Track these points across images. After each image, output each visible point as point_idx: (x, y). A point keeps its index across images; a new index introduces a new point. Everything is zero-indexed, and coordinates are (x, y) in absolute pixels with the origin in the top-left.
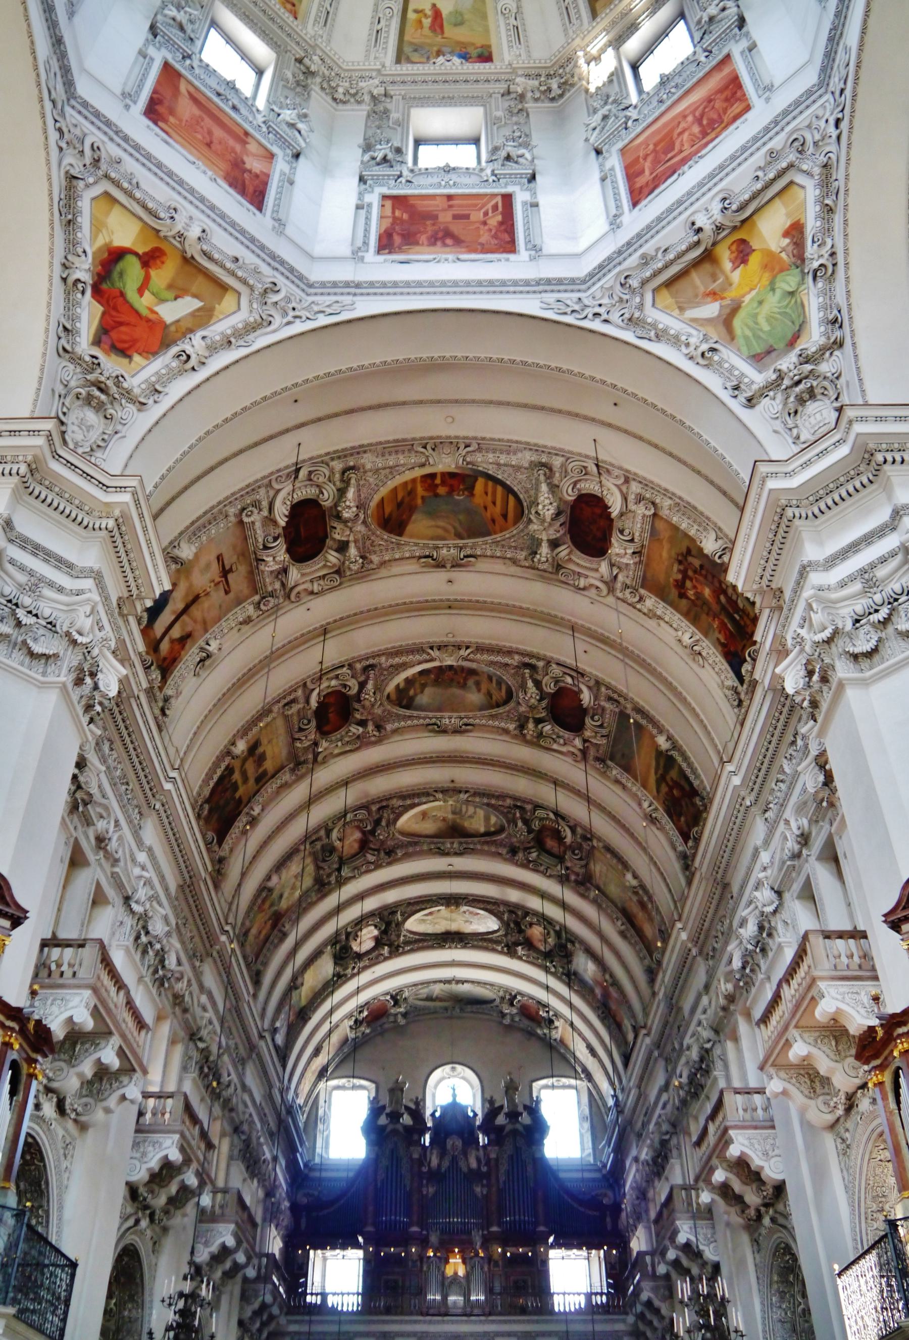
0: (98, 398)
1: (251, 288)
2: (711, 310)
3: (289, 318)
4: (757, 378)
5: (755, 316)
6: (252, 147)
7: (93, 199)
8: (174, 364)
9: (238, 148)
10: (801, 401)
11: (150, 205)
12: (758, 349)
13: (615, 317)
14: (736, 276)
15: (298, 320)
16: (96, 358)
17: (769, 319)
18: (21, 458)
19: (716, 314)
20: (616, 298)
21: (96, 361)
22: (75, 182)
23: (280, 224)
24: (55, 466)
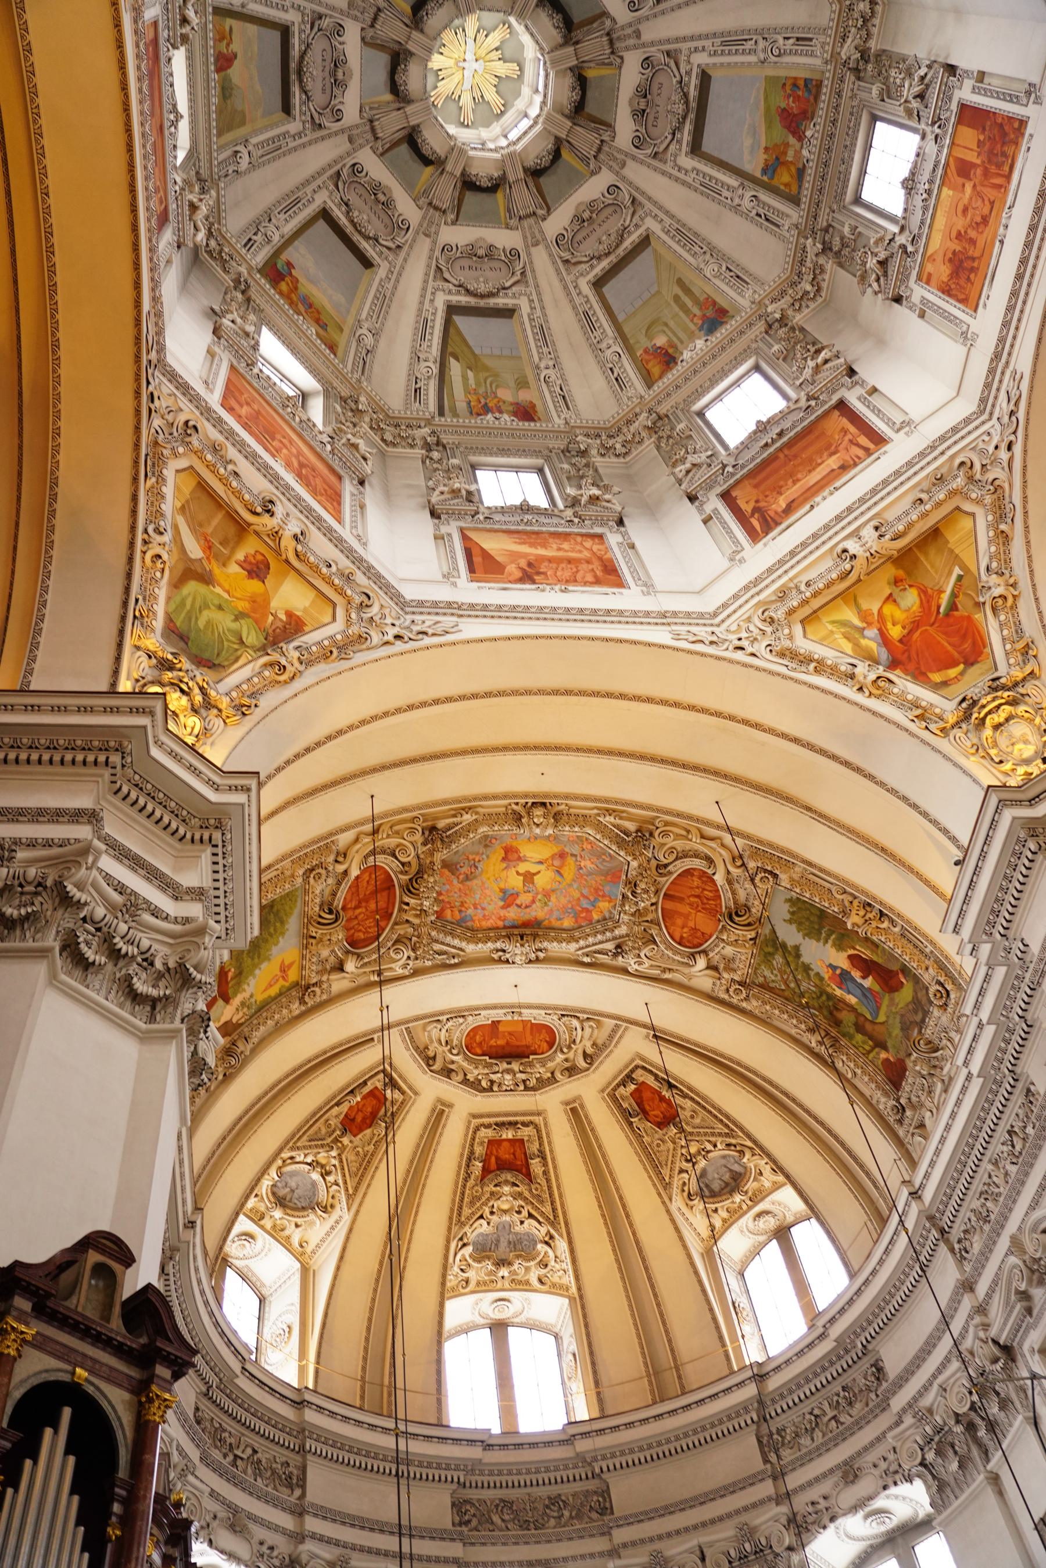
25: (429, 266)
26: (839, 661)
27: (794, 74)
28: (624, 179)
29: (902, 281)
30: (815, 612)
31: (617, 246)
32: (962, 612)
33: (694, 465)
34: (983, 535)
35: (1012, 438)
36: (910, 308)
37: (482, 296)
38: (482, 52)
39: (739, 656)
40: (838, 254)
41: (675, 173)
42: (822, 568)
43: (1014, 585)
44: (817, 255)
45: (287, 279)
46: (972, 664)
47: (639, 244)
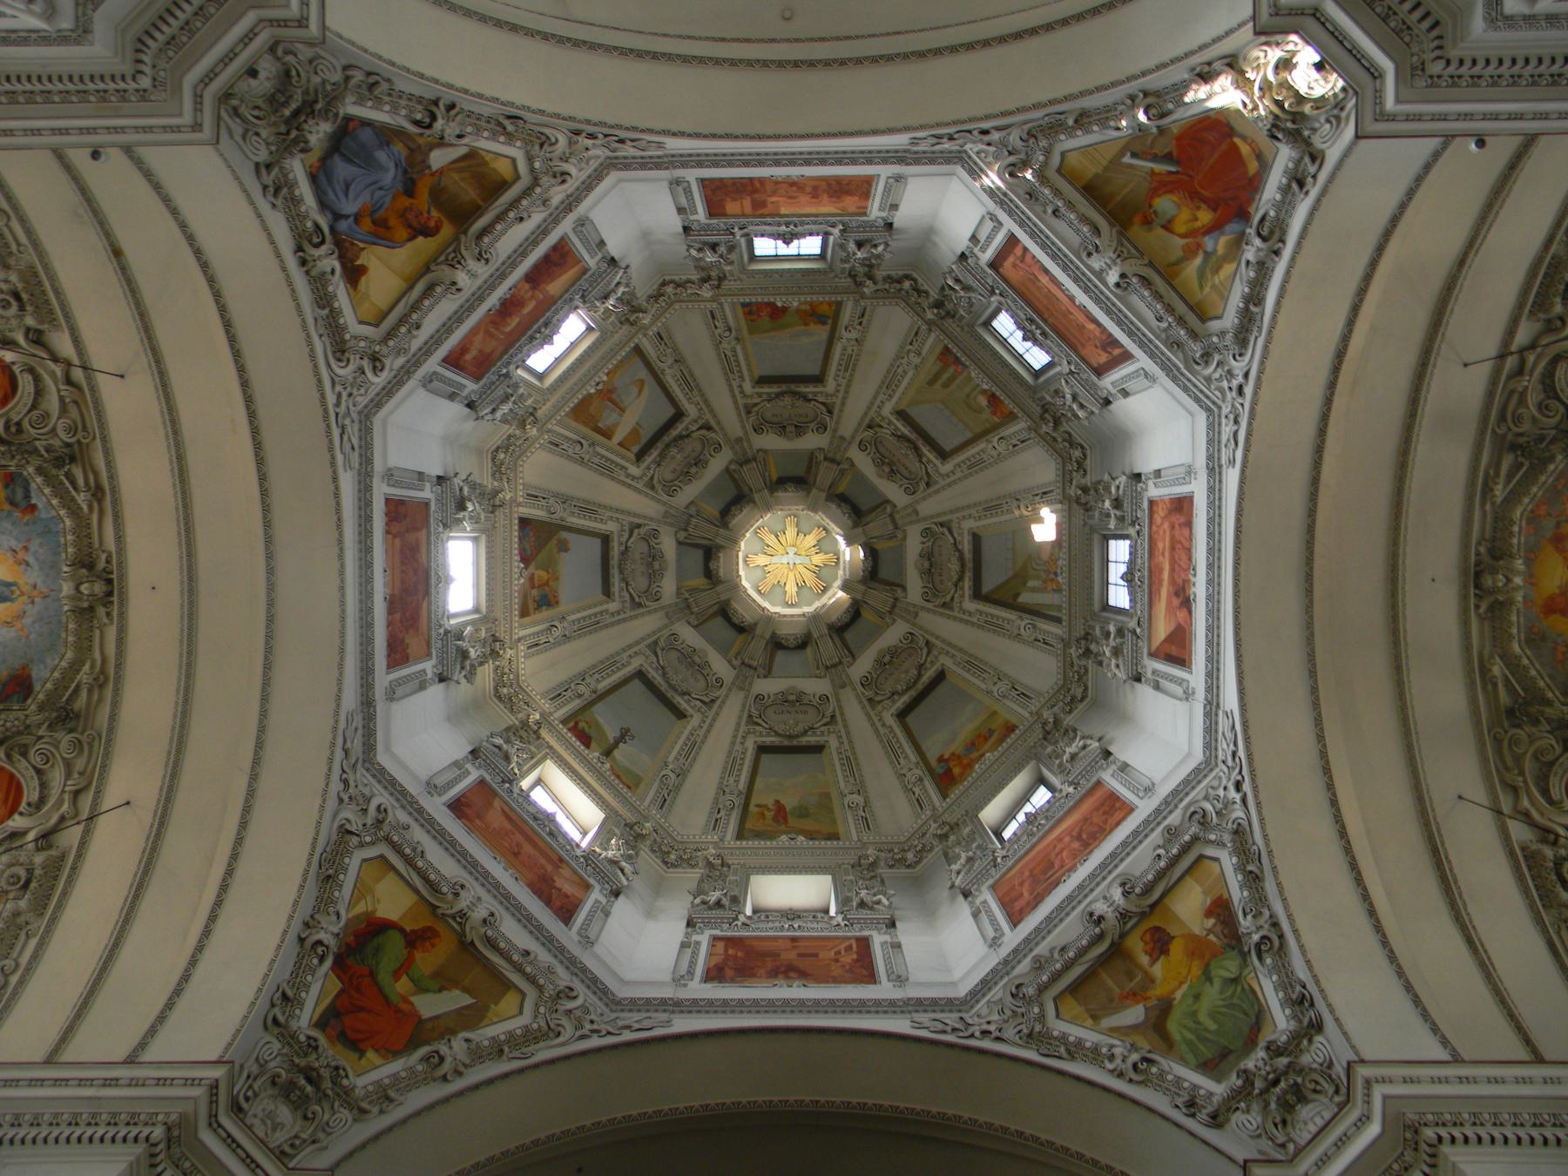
0: (302, 1089)
1: (540, 988)
2: (1134, 1014)
3: (585, 1031)
4: (1215, 1089)
5: (1193, 1015)
6: (565, 872)
7: (364, 860)
8: (420, 1068)
9: (549, 868)
10: (1287, 1107)
11: (432, 877)
12: (1207, 1053)
13: (1010, 1033)
14: (1157, 970)
15: (595, 1035)
16: (315, 1040)
17: (1213, 1015)
18: (160, 1117)
19: (1142, 1018)
20: (1008, 1013)
21: (313, 1044)
22: (348, 837)
23: (588, 942)
24: (208, 1138)
33: (1075, 397)
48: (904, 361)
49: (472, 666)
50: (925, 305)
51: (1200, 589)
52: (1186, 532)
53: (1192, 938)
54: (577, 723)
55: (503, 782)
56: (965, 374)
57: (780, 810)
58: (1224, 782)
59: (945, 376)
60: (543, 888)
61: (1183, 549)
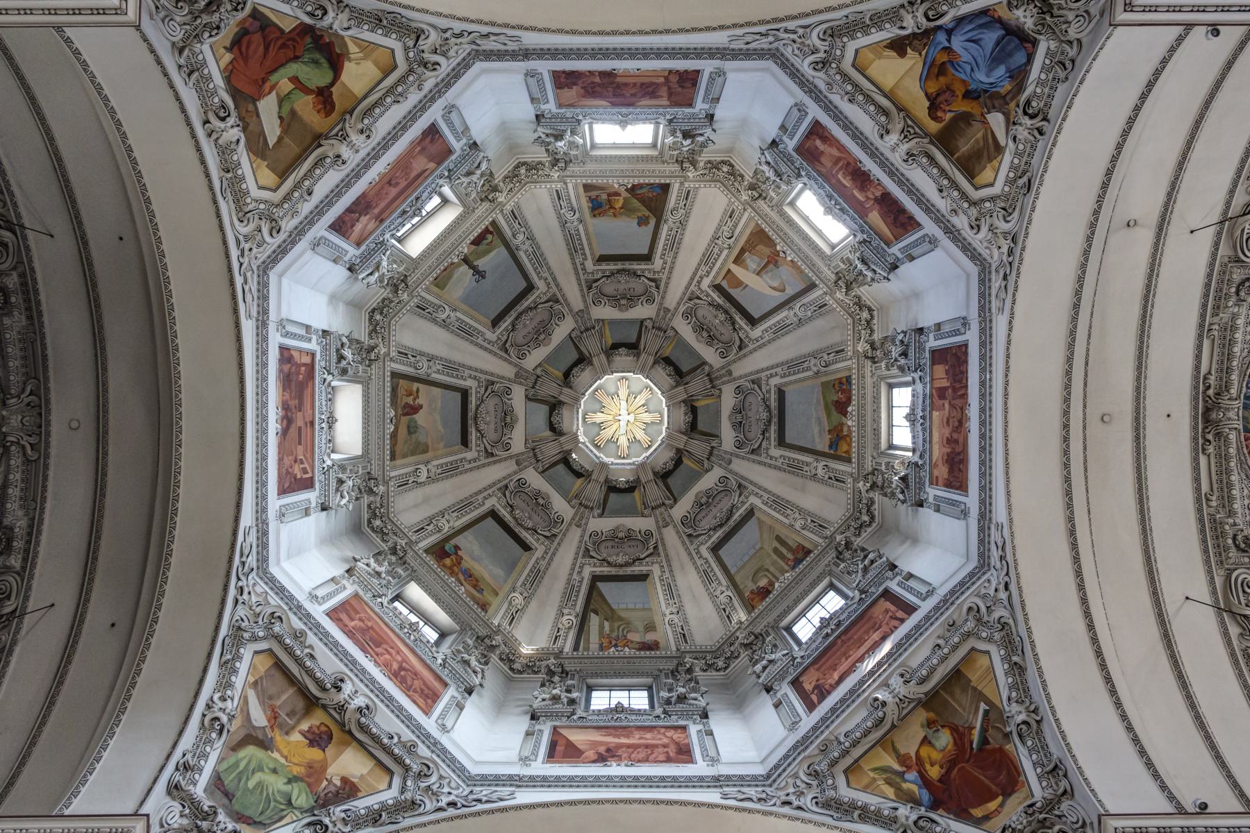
11: (377, 111)
14: (296, 737)
25: (579, 548)
26: (882, 806)
27: (839, 376)
28: (731, 471)
29: (920, 489)
30: (856, 761)
31: (728, 519)
32: (994, 744)
33: (770, 662)
34: (1000, 669)
35: (1007, 579)
36: (929, 507)
37: (621, 566)
38: (632, 408)
39: (786, 810)
40: (882, 488)
41: (768, 461)
42: (857, 719)
43: (1035, 711)
44: (867, 491)
45: (453, 557)
46: (1010, 795)
47: (746, 516)
48: (797, 515)
49: (549, 144)
50: (847, 534)
51: (615, 769)
52: (662, 757)
53: (324, 767)
54: (491, 233)
55: (449, 171)
56: (786, 568)
57: (415, 409)
58: (455, 792)
59: (784, 551)
60: (361, 206)
61: (647, 754)
